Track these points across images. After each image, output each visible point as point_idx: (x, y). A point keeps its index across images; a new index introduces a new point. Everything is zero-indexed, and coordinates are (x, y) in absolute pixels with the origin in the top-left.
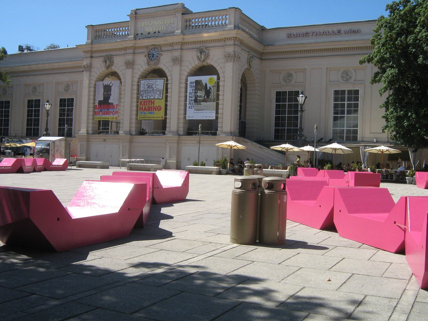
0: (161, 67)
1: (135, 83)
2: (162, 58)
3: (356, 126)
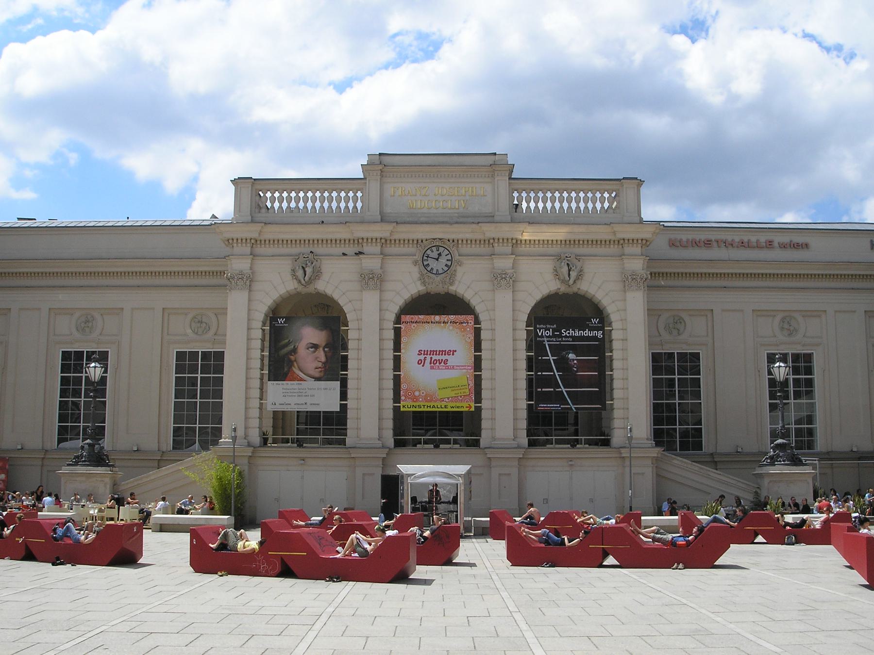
0: (329, 291)
1: (390, 325)
2: (460, 271)
3: (699, 422)
